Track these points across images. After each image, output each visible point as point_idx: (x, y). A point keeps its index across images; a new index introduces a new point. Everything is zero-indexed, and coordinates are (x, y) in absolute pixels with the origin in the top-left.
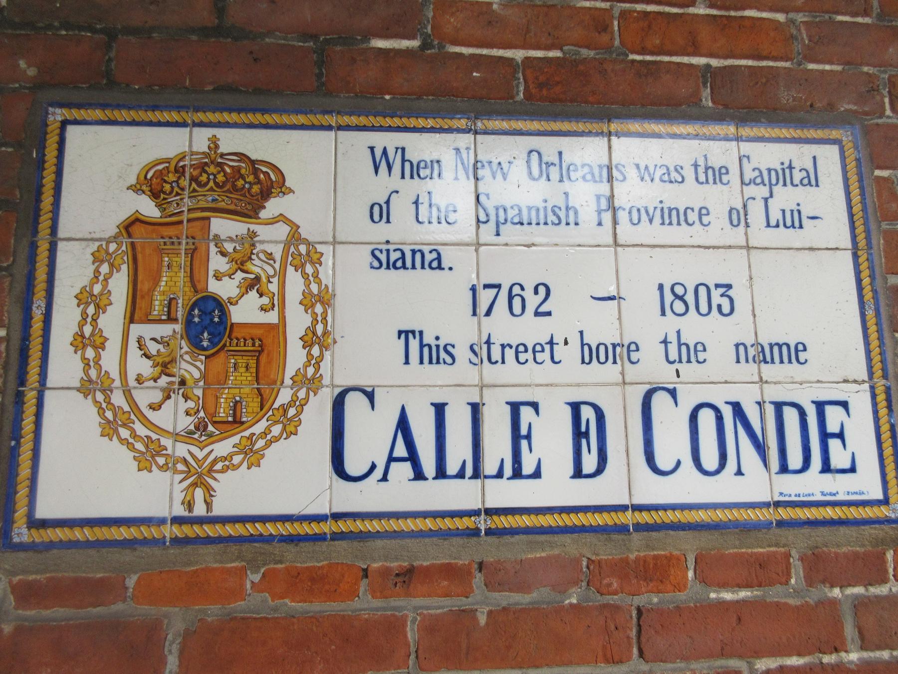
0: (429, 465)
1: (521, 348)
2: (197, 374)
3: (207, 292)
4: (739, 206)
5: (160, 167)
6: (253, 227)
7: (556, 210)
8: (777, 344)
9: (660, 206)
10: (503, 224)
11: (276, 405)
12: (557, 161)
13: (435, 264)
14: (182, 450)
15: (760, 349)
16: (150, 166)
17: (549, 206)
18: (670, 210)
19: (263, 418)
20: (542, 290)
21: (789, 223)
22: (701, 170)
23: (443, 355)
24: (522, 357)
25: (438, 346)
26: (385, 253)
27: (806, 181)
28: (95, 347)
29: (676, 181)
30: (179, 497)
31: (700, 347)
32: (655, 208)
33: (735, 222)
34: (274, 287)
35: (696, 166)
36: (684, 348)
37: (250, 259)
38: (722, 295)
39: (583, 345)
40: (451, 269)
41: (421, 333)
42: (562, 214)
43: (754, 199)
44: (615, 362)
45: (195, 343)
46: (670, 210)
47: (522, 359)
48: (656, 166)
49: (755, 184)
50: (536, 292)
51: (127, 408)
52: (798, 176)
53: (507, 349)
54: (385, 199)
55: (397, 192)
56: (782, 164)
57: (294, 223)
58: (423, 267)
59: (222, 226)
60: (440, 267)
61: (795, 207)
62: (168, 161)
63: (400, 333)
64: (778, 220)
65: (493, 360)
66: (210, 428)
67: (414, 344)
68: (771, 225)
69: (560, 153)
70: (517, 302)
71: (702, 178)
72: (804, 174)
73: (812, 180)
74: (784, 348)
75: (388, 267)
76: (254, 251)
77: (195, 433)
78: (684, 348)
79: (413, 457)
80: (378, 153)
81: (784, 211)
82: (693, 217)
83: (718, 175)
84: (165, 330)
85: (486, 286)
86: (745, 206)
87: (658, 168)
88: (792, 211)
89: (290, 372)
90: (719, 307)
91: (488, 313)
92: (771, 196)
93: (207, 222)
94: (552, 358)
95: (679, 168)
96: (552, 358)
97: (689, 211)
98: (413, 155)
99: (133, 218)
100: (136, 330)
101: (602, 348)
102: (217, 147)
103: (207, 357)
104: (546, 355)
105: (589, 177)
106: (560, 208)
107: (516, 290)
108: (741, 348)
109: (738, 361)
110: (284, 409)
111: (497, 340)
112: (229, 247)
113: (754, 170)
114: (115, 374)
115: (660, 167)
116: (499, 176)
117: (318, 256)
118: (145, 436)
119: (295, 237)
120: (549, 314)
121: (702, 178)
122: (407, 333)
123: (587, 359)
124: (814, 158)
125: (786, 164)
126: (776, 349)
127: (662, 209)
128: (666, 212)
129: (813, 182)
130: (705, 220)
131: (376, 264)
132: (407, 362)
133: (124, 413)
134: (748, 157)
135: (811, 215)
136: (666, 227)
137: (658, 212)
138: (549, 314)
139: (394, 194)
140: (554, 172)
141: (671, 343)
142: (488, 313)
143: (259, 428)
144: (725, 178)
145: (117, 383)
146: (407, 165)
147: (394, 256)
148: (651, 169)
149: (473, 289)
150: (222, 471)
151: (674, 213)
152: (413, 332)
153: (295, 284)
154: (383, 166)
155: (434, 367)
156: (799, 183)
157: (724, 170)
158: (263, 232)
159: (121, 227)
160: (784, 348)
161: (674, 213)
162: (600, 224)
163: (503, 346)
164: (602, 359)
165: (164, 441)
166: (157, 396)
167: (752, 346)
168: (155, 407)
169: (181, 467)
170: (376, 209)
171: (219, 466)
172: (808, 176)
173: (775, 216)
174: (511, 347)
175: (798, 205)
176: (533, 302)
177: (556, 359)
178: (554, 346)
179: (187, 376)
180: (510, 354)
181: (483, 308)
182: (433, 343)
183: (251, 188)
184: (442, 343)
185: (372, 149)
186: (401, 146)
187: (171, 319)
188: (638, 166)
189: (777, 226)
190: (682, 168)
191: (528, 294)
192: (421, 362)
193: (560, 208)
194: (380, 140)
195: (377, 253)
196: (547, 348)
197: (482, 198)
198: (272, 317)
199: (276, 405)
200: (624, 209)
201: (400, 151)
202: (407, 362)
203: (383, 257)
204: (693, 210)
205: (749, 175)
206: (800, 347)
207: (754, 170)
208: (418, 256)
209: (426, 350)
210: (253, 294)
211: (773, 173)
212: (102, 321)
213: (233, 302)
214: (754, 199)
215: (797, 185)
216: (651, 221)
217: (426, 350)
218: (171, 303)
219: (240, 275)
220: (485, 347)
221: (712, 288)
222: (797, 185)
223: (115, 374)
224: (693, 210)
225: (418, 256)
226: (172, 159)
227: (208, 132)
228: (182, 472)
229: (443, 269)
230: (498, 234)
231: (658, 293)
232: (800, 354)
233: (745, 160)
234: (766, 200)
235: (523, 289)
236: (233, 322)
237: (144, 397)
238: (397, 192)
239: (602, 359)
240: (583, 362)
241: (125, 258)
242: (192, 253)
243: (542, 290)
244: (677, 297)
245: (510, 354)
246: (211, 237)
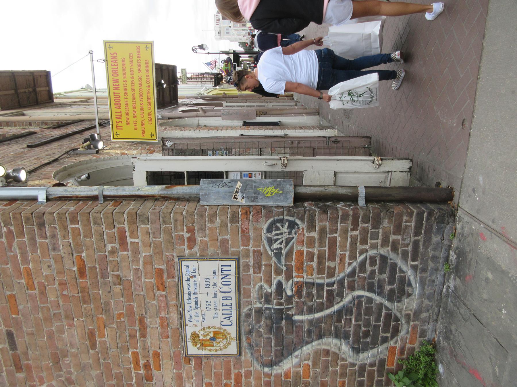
0: (231, 315)
14: (228, 341)
45: (215, 340)
73: (188, 266)
79: (230, 317)
82: (195, 283)
84: (214, 343)
119: (201, 330)
153: (207, 330)
158: (201, 334)
173: (194, 272)
198: (212, 332)
237: (222, 345)
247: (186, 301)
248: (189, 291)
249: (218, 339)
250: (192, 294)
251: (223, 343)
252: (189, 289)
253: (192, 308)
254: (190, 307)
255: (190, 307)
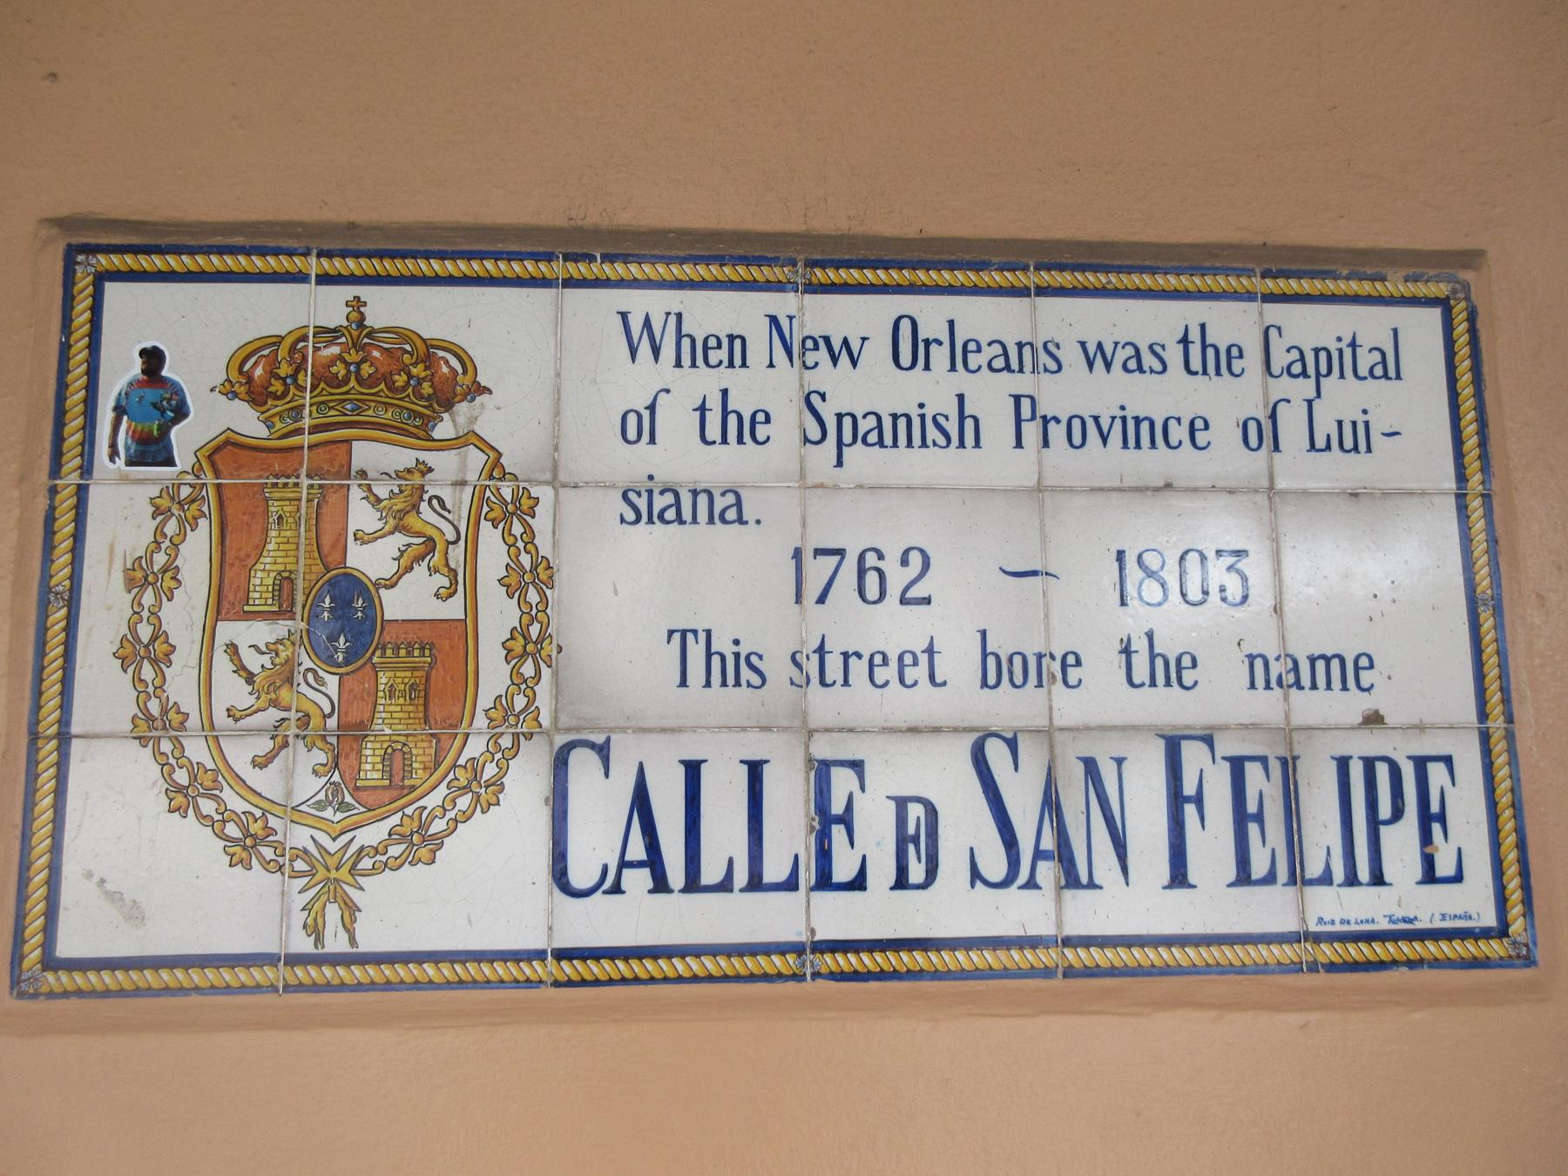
1: (878, 659)
2: (327, 710)
3: (345, 567)
4: (1262, 415)
5: (266, 352)
6: (423, 456)
7: (941, 420)
8: (1322, 657)
9: (1121, 413)
10: (847, 445)
11: (462, 761)
12: (945, 339)
13: (731, 514)
15: (1290, 665)
16: (250, 348)
17: (929, 412)
18: (1138, 421)
19: (443, 781)
20: (915, 558)
21: (1348, 444)
22: (1195, 350)
23: (746, 673)
24: (881, 674)
25: (737, 655)
26: (645, 495)
27: (1378, 371)
28: (155, 662)
29: (1152, 371)
30: (299, 918)
31: (1186, 661)
32: (1113, 418)
33: (1254, 442)
34: (457, 554)
35: (1185, 341)
36: (1159, 663)
37: (415, 508)
38: (1230, 568)
39: (985, 655)
40: (758, 522)
41: (708, 633)
42: (952, 427)
43: (1289, 401)
44: (1040, 685)
46: (1138, 421)
47: (879, 680)
48: (1116, 344)
49: (1290, 374)
50: (904, 562)
51: (210, 765)
52: (1366, 360)
53: (853, 660)
54: (648, 403)
55: (668, 391)
56: (1339, 339)
57: (493, 448)
58: (711, 521)
59: (370, 454)
60: (741, 520)
61: (1360, 419)
62: (278, 341)
63: (671, 633)
64: (1328, 436)
65: (829, 680)
66: (348, 799)
67: (696, 652)
68: (1317, 447)
69: (951, 323)
70: (872, 579)
71: (1196, 364)
72: (1377, 357)
73: (1388, 368)
74: (1335, 664)
75: (650, 521)
76: (426, 497)
77: (320, 806)
78: (1159, 663)
80: (636, 325)
81: (1340, 423)
82: (1178, 433)
83: (1224, 361)
85: (818, 552)
86: (1273, 416)
87: (1120, 346)
88: (1354, 424)
89: (485, 701)
90: (1222, 589)
91: (821, 600)
92: (1319, 395)
93: (345, 447)
94: (932, 677)
95: (1158, 349)
96: (932, 677)
97: (1172, 423)
98: (697, 327)
99: (222, 437)
100: (228, 631)
101: (1018, 660)
102: (362, 317)
103: (341, 676)
104: (920, 672)
105: (999, 363)
106: (947, 418)
107: (871, 559)
108: (1259, 663)
109: (1253, 686)
110: (475, 768)
111: (835, 646)
112: (382, 491)
113: (1288, 351)
114: (190, 704)
115: (1123, 347)
116: (844, 359)
117: (531, 502)
118: (243, 813)
120: (927, 601)
121: (1196, 364)
122: (684, 633)
123: (992, 680)
124: (1395, 331)
125: (1347, 339)
126: (1320, 665)
127: (1124, 419)
128: (1131, 425)
129: (1392, 372)
130: (1201, 438)
131: (631, 516)
132: (683, 683)
133: (206, 771)
134: (1279, 329)
135: (1387, 431)
136: (1132, 452)
137: (1118, 423)
138: (927, 601)
139: (663, 394)
140: (940, 355)
141: (1137, 652)
142: (821, 600)
143: (433, 800)
144: (1237, 365)
145: (194, 721)
146: (686, 342)
147: (660, 502)
148: (1109, 350)
149: (798, 554)
150: (374, 870)
151: (1145, 426)
152: (695, 632)
154: (645, 349)
155: (730, 689)
156: (1367, 375)
157: (1234, 352)
159: (197, 453)
160: (1335, 664)
161: (1145, 426)
162: (1019, 444)
163: (846, 656)
164: (1018, 680)
165: (273, 822)
166: (264, 745)
167: (1277, 659)
168: (260, 763)
169: (300, 865)
170: (632, 419)
171: (366, 863)
172: (1384, 362)
173: (1325, 427)
174: (859, 656)
175: (1365, 412)
176: (897, 578)
177: (939, 680)
178: (935, 655)
179: (312, 710)
180: (858, 668)
181: (813, 589)
182: (728, 650)
183: (420, 384)
184: (744, 650)
185: (624, 316)
186: (677, 311)
187: (285, 612)
188: (1083, 344)
189: (1328, 447)
190: (1163, 347)
191: (891, 566)
192: (708, 684)
193: (947, 418)
194: (640, 303)
195: (632, 496)
196: (923, 659)
197: (815, 399)
198: (453, 609)
199: (462, 761)
200: (1058, 421)
201: (672, 320)
202: (683, 683)
203: (642, 504)
204: (1179, 420)
205: (1280, 359)
206: (1364, 662)
207: (1288, 351)
208: (703, 500)
209: (716, 660)
210: (421, 570)
211: (1323, 355)
212: (168, 612)
213: (391, 584)
214: (1289, 401)
215: (1365, 378)
216: (1105, 440)
217: (716, 660)
218: (284, 583)
219: (399, 540)
220: (815, 658)
221: (1211, 555)
222: (1365, 378)
223: (190, 704)
224: (1179, 420)
225: (703, 500)
226: (283, 338)
227: (349, 292)
228: (301, 874)
229: (747, 523)
230: (840, 463)
231: (1116, 565)
232: (1362, 673)
233: (1273, 333)
234: (1310, 402)
235: (881, 557)
236: (386, 617)
238: (668, 391)
239: (1018, 680)
240: (984, 684)
241: (205, 509)
242: (321, 497)
243: (915, 558)
244: (1150, 574)
245: (858, 668)
246: (353, 473)
247: (932, 313)
248: (1071, 356)
249: (332, 683)
250: (1022, 383)
251: (260, 763)
252: (1097, 356)
253: (827, 377)
254: (845, 352)
255: (845, 352)
